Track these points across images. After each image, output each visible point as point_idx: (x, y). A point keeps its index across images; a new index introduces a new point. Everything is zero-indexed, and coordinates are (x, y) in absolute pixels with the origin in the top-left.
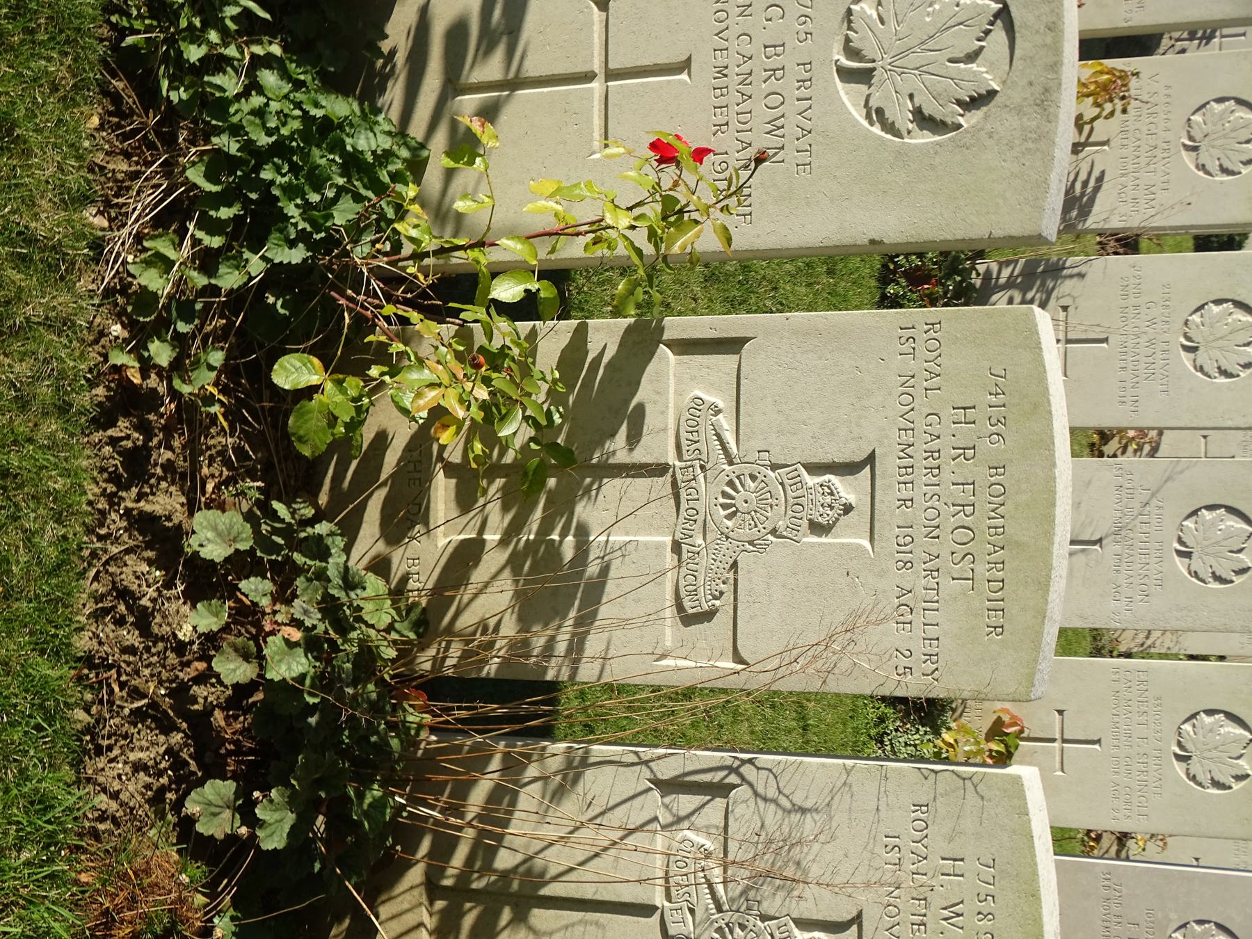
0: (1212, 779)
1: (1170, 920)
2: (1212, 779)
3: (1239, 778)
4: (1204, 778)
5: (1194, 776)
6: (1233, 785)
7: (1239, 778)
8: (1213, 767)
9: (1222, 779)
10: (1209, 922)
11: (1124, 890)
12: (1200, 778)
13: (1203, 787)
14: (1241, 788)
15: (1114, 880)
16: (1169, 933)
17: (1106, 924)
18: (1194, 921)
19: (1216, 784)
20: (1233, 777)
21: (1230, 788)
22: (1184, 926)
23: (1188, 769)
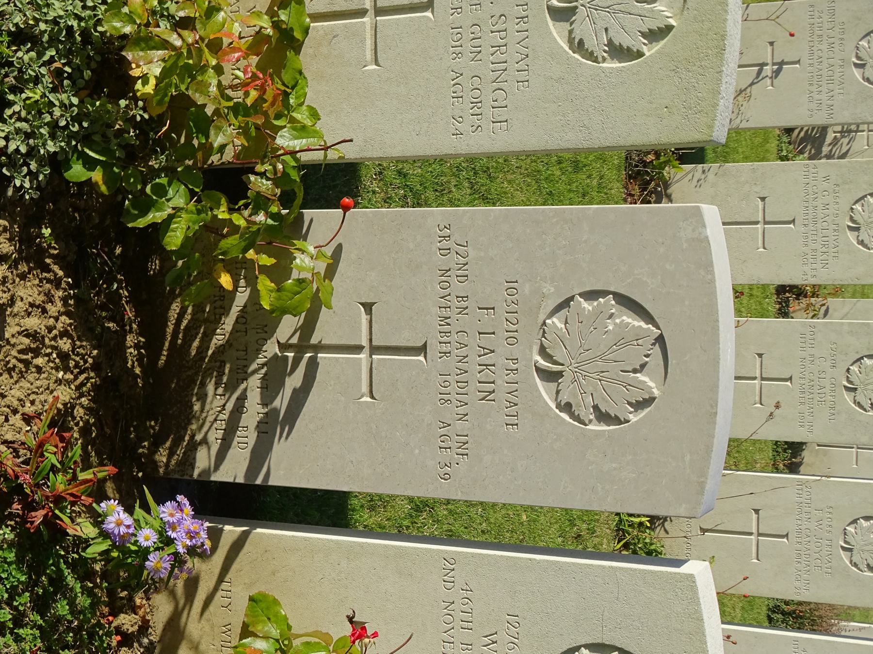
0: (610, 43)
1: (544, 296)
2: (610, 43)
3: (655, 35)
4: (596, 43)
5: (581, 42)
6: (645, 49)
7: (655, 35)
8: (611, 22)
9: (626, 41)
10: (603, 293)
11: (472, 253)
12: (591, 44)
13: (596, 60)
14: (657, 52)
15: (457, 237)
16: (542, 317)
17: (444, 313)
18: (581, 295)
19: (619, 52)
20: (644, 35)
21: (640, 54)
22: (565, 304)
23: (571, 32)
